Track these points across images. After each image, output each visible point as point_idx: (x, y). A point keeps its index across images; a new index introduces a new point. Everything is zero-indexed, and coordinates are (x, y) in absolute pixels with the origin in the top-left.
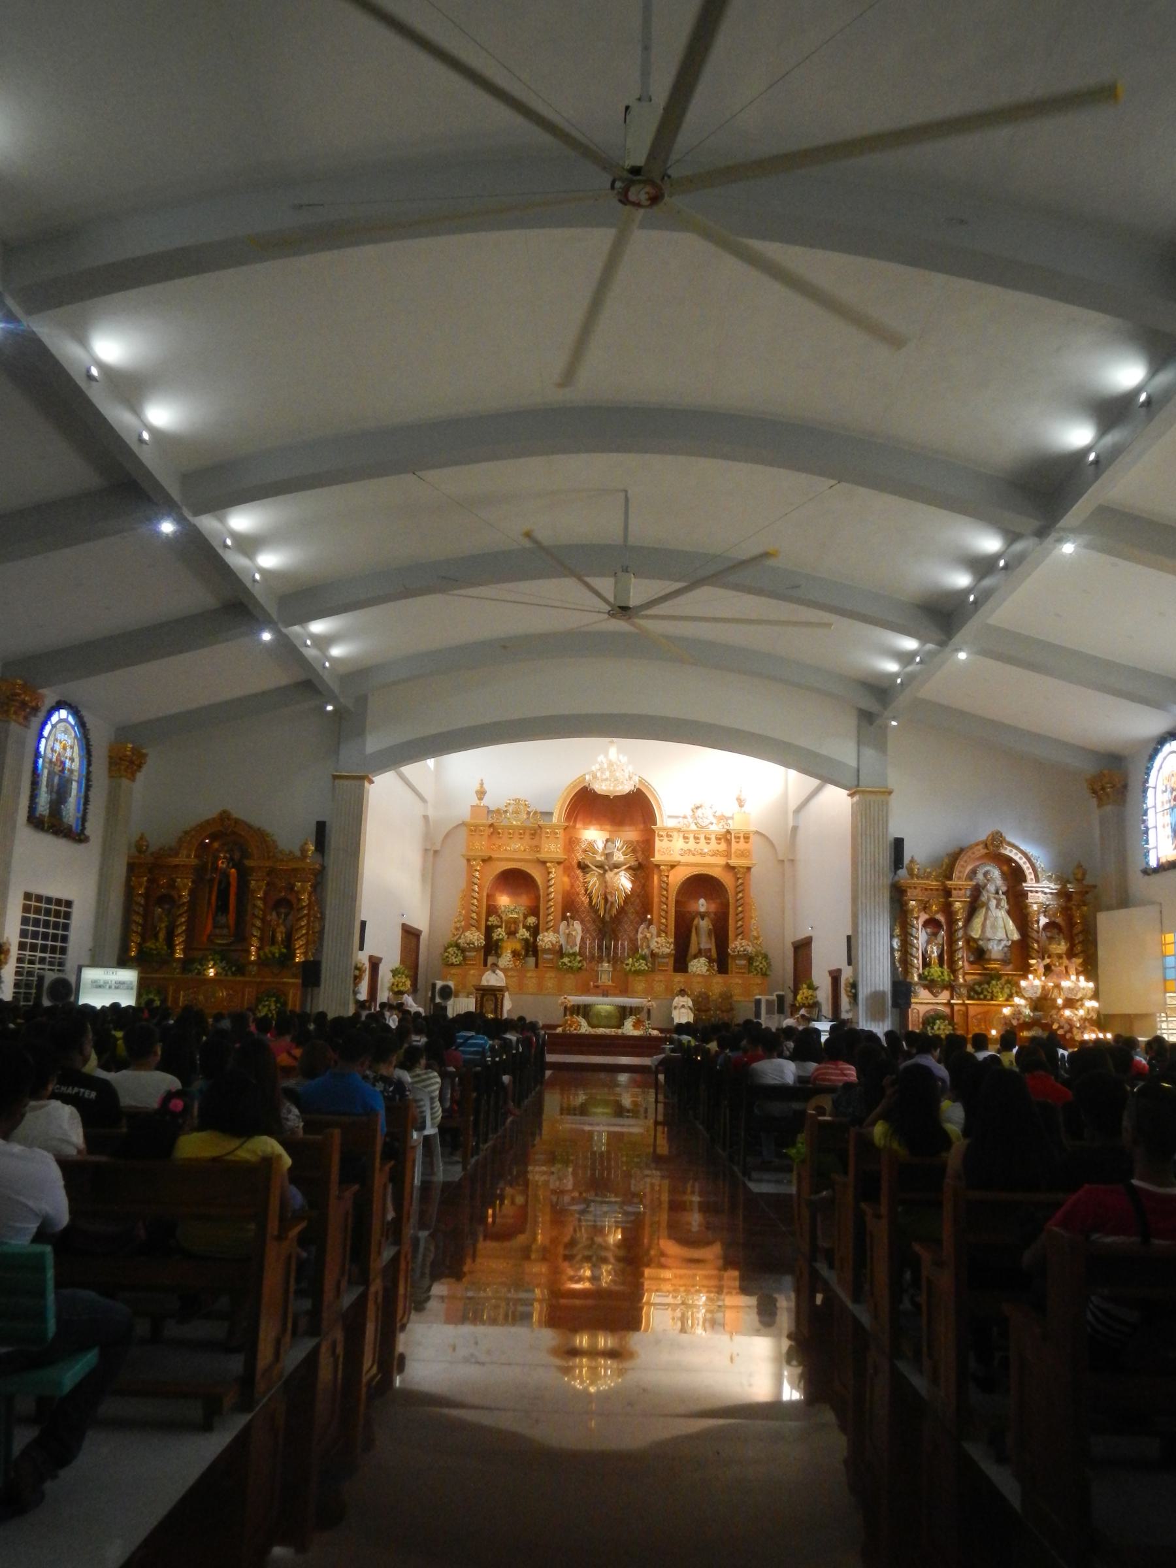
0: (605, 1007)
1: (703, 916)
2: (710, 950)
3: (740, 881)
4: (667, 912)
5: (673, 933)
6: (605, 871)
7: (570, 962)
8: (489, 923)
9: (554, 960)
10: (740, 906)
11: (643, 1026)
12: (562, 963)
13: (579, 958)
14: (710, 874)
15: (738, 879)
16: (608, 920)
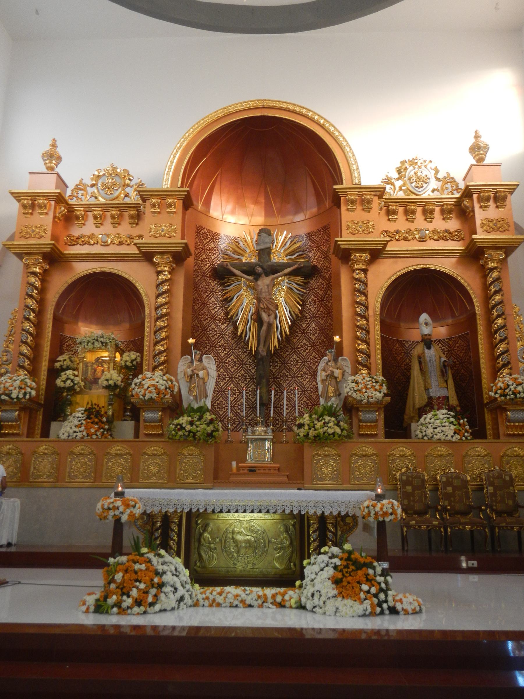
0: (248, 516)
1: (428, 342)
2: (447, 398)
3: (495, 274)
4: (368, 332)
5: (380, 371)
6: (257, 277)
7: (191, 423)
8: (57, 365)
9: (167, 420)
10: (498, 316)
11: (369, 580)
12: (176, 426)
13: (208, 416)
14: (438, 268)
15: (492, 269)
16: (265, 354)
